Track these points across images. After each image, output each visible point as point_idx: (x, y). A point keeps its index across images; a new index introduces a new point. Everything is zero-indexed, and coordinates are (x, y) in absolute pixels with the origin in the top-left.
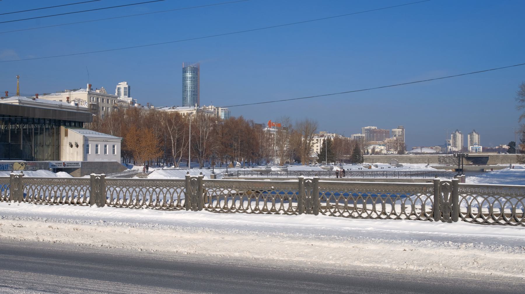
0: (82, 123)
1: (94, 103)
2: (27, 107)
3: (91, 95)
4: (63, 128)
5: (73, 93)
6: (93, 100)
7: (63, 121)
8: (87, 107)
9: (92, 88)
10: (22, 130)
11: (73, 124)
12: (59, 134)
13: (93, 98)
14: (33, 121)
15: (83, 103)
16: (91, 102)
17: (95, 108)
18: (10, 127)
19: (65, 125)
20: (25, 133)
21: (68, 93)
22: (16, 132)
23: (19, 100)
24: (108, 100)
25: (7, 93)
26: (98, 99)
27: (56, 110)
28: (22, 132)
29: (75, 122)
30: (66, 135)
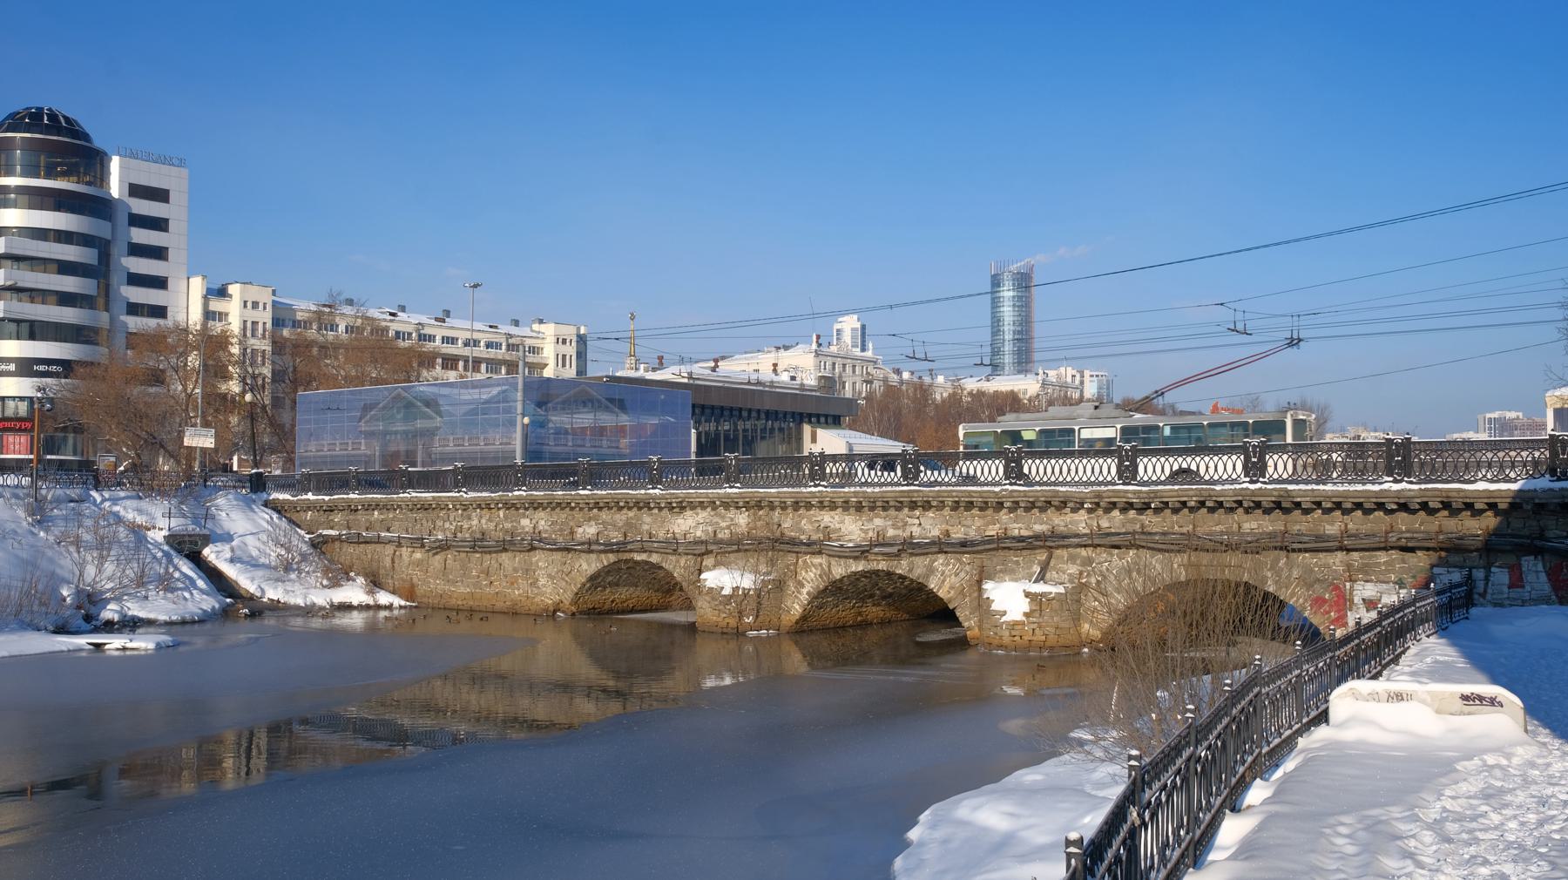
0: (839, 416)
1: (827, 375)
2: (705, 386)
3: (823, 359)
4: (807, 429)
6: (825, 369)
7: (807, 414)
9: (820, 341)
10: (741, 432)
11: (822, 419)
13: (825, 363)
14: (735, 413)
17: (828, 383)
19: (810, 422)
21: (773, 355)
22: (732, 436)
24: (854, 366)
25: (661, 358)
27: (796, 394)
29: (826, 416)
30: (814, 440)
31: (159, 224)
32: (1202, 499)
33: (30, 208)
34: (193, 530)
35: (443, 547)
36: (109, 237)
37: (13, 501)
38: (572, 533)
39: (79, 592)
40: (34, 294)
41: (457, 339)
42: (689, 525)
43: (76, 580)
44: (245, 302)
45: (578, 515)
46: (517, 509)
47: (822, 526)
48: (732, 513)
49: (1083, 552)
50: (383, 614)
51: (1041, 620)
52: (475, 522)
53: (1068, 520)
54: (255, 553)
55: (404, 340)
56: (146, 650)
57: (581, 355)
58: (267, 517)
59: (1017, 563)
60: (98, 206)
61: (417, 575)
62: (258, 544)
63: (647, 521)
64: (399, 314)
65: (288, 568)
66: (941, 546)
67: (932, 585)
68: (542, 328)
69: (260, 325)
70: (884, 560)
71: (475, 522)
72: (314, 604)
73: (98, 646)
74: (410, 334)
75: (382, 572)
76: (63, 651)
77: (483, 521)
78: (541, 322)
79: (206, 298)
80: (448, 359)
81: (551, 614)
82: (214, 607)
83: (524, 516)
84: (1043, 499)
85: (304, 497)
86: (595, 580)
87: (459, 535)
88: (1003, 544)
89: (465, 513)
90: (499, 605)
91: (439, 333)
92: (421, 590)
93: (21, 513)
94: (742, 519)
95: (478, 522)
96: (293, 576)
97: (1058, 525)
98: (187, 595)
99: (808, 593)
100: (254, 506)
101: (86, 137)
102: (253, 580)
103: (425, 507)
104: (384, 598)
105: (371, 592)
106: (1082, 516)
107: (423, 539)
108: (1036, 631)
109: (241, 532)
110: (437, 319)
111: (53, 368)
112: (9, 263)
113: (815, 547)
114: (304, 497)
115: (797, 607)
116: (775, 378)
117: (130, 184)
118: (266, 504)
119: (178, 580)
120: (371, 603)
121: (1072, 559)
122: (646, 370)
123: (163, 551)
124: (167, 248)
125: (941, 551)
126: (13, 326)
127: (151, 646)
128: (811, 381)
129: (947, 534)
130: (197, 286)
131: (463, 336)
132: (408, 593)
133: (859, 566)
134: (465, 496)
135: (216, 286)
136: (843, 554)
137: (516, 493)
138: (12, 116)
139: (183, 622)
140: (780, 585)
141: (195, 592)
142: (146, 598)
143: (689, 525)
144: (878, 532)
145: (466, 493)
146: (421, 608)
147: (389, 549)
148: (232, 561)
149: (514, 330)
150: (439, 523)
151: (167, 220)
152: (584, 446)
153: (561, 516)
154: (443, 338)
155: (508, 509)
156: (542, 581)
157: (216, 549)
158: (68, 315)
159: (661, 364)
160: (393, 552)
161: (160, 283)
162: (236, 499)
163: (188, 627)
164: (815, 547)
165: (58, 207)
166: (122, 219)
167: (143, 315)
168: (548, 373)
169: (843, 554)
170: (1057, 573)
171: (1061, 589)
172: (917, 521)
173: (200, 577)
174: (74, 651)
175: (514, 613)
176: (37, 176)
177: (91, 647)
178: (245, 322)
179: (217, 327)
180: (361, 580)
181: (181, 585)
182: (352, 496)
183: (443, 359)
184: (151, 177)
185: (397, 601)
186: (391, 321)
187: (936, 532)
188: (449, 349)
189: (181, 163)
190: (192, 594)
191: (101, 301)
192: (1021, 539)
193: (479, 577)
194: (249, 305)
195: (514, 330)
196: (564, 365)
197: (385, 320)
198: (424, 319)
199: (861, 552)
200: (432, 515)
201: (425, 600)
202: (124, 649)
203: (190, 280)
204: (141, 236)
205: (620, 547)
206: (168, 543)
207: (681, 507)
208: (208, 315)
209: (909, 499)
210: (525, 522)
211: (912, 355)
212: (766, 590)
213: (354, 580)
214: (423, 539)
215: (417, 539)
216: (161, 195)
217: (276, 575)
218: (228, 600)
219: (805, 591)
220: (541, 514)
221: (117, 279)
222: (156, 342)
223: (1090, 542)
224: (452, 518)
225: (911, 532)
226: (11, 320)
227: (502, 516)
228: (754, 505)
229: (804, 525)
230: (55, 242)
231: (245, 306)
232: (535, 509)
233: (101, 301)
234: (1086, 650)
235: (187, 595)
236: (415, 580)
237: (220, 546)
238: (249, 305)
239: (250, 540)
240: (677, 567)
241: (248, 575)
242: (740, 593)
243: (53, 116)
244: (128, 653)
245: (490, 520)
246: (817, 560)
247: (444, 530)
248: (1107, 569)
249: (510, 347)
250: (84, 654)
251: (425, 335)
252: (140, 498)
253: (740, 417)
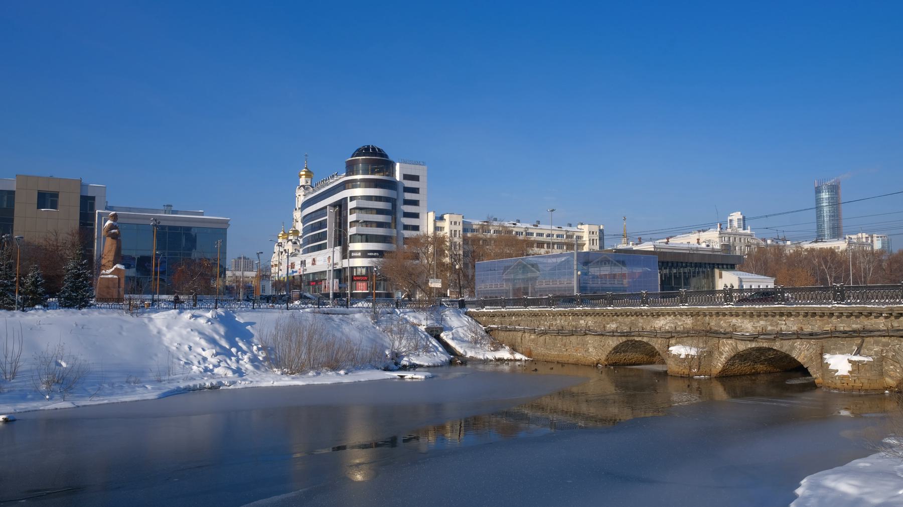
0: (734, 265)
5: (702, 233)
6: (725, 240)
8: (718, 248)
9: (721, 227)
10: (682, 273)
12: (713, 276)
15: (714, 244)
16: (722, 242)
17: (727, 247)
18: (682, 270)
19: (718, 268)
20: (675, 277)
23: (654, 246)
24: (740, 239)
26: (729, 238)
28: (682, 276)
29: (727, 265)
30: (721, 277)
31: (415, 191)
33: (365, 188)
34: (437, 325)
35: (544, 333)
36: (396, 198)
37: (366, 314)
38: (604, 327)
39: (392, 353)
40: (367, 223)
41: (543, 234)
42: (662, 323)
43: (391, 347)
44: (451, 222)
45: (607, 319)
46: (578, 316)
47: (732, 324)
48: (684, 318)
49: (884, 340)
50: (518, 363)
51: (859, 375)
52: (558, 322)
53: (873, 322)
54: (462, 335)
55: (519, 235)
56: (421, 379)
57: (601, 239)
58: (466, 319)
59: (843, 345)
60: (390, 185)
61: (532, 346)
62: (463, 331)
63: (641, 322)
64: (517, 224)
65: (476, 342)
66: (798, 335)
67: (794, 355)
68: (583, 227)
69: (458, 231)
70: (766, 342)
71: (558, 322)
72: (488, 358)
73: (402, 377)
74: (522, 233)
75: (517, 344)
76: (388, 379)
77: (562, 321)
78: (582, 224)
79: (435, 221)
80: (539, 243)
81: (595, 365)
82: (446, 360)
83: (581, 319)
84: (858, 311)
85: (482, 310)
86: (616, 350)
87: (551, 328)
88: (833, 334)
89: (554, 318)
90: (571, 361)
91: (535, 232)
92: (534, 352)
93: (369, 319)
94: (689, 322)
95: (559, 322)
96: (478, 346)
97: (867, 325)
98: (435, 354)
99: (725, 358)
100: (461, 315)
101: (386, 156)
102: (461, 347)
103: (535, 315)
104: (518, 356)
105: (512, 354)
106: (881, 320)
107: (535, 329)
109: (456, 326)
110: (534, 225)
111: (375, 254)
112: (358, 211)
113: (728, 335)
114: (482, 310)
115: (720, 365)
116: (699, 246)
117: (404, 175)
118: (466, 313)
119: (431, 347)
120: (513, 358)
121: (877, 343)
122: (633, 245)
123: (425, 335)
124: (419, 201)
125: (798, 338)
126: (359, 237)
127: (423, 377)
128: (717, 247)
129: (802, 329)
130: (431, 216)
131: (546, 233)
132: (529, 354)
133: (754, 345)
134: (554, 310)
135: (439, 216)
136: (743, 339)
137: (577, 308)
138: (358, 150)
139: (434, 366)
140: (710, 354)
141: (438, 353)
142: (419, 355)
143: (662, 323)
144: (762, 328)
145: (554, 308)
146: (534, 362)
147: (520, 334)
148: (453, 339)
149: (569, 229)
150: (542, 322)
151: (418, 189)
152: (606, 284)
153: (599, 319)
154: (537, 234)
155: (574, 316)
156: (591, 350)
157: (446, 334)
158: (380, 231)
159: (640, 241)
160: (521, 335)
161: (416, 216)
162: (453, 312)
163: (436, 368)
164: (728, 335)
165: (376, 187)
166: (401, 189)
167: (410, 230)
168: (586, 249)
169: (743, 339)
170: (867, 350)
171: (871, 359)
173: (440, 346)
174: (393, 379)
175: (576, 364)
176: (368, 174)
177: (399, 377)
178: (451, 230)
179: (440, 234)
180: (507, 348)
181: (432, 350)
182: (502, 310)
183: (537, 244)
184: (412, 170)
185: (524, 358)
186: (514, 227)
187: (795, 328)
188: (540, 239)
189: (424, 164)
190: (437, 354)
191: (393, 225)
192: (845, 332)
193: (561, 347)
194: (453, 223)
195: (569, 229)
196: (593, 244)
197: (511, 227)
198: (528, 226)
199: (754, 338)
200: (539, 318)
201: (536, 357)
202: (412, 378)
203: (429, 214)
204: (409, 196)
205: (628, 334)
206: (426, 331)
207: (658, 315)
208: (436, 228)
209: (779, 311)
210: (582, 322)
211: (777, 238)
212: (703, 356)
213: (505, 348)
214: (535, 329)
215: (532, 329)
216: (415, 178)
217: (471, 345)
218: (452, 356)
219: (724, 357)
220: (589, 318)
221: (399, 214)
222: (415, 241)
223: (887, 334)
224: (548, 320)
226: (359, 235)
227: (571, 319)
228: (694, 314)
229: (723, 324)
230: (375, 201)
231: (451, 224)
232: (587, 316)
233: (393, 225)
234: (887, 392)
235: (435, 354)
236: (532, 348)
237: (447, 333)
238: (453, 223)
239: (460, 330)
240: (657, 344)
241: (460, 345)
242: (690, 357)
243: (373, 149)
244: (414, 380)
245: (565, 321)
246: (730, 341)
247: (544, 326)
248: (899, 349)
249: (568, 237)
250: (396, 380)
251: (529, 233)
252: (415, 312)
253: (682, 267)
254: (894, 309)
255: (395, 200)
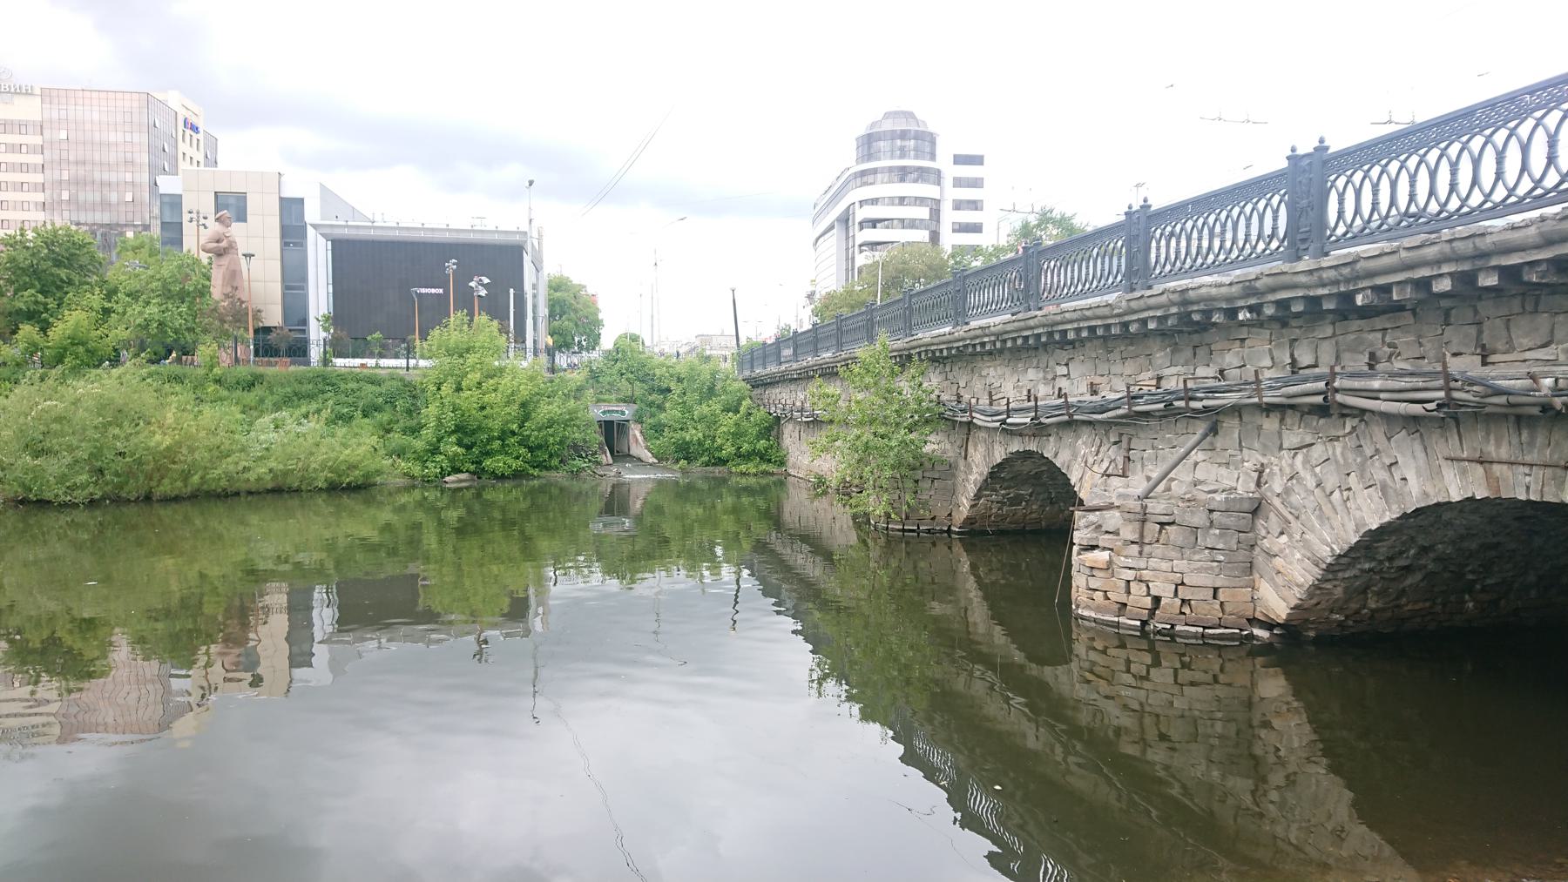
32: (1466, 267)
108: (1131, 584)
115: (965, 501)
172: (1064, 370)
225: (1060, 389)
254: (1258, 284)
255: (938, 202)
